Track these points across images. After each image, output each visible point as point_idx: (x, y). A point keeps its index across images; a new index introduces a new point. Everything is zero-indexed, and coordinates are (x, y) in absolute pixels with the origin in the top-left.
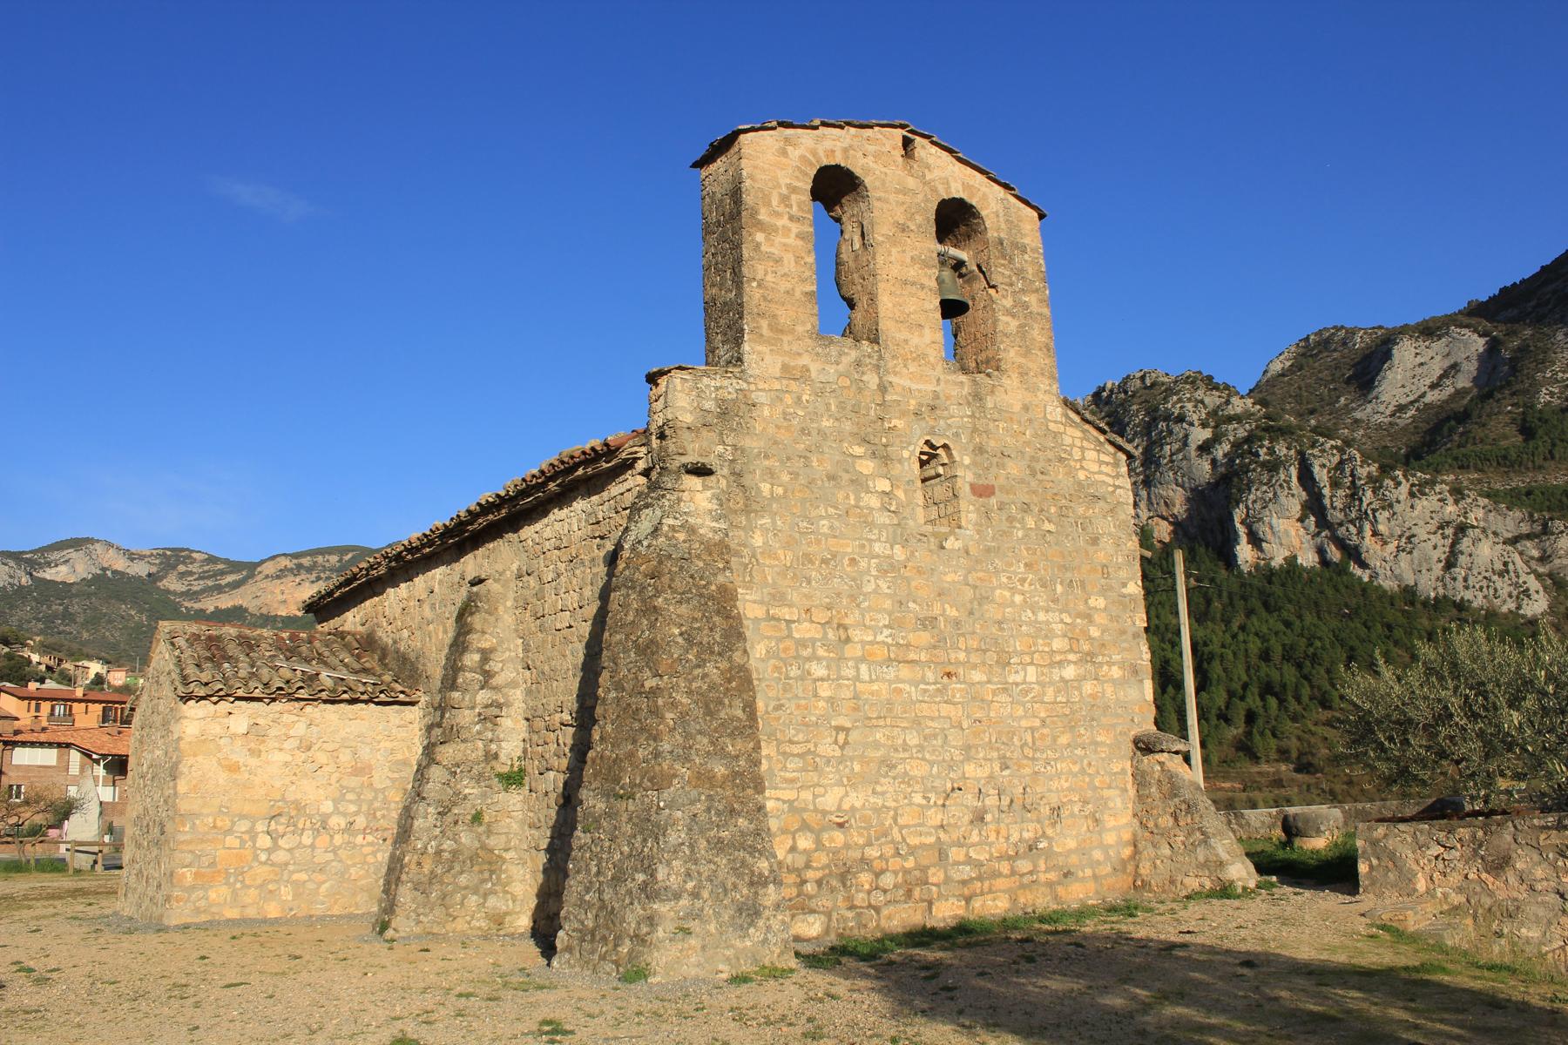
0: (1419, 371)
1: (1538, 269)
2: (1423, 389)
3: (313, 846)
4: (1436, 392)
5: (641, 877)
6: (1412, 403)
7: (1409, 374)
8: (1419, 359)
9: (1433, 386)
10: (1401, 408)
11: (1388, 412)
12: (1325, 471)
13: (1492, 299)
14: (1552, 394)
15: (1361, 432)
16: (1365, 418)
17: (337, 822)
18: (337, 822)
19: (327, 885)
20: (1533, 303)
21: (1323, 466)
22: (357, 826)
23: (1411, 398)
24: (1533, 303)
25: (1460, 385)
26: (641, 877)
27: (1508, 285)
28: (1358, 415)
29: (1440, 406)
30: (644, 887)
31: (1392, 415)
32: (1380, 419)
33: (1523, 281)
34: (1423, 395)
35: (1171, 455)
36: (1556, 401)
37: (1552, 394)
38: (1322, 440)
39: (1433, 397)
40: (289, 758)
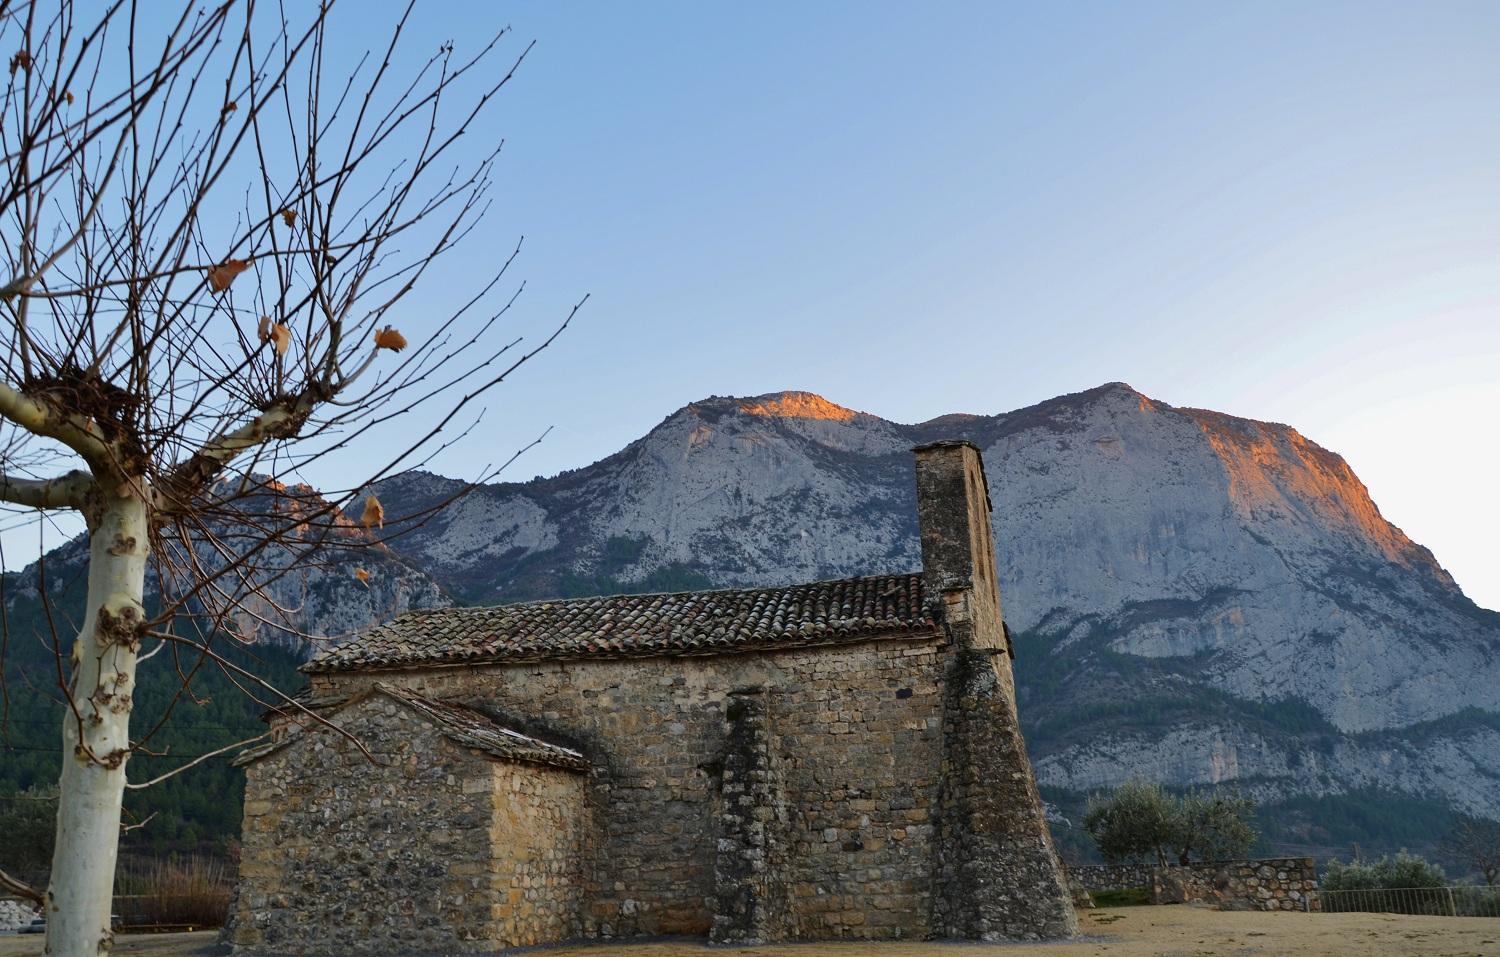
0: (486, 524)
1: (591, 463)
2: (486, 542)
3: (545, 887)
4: (497, 546)
5: (1043, 884)
6: (476, 551)
7: (478, 526)
8: (488, 516)
9: (496, 541)
10: (467, 554)
11: (455, 555)
12: (408, 598)
13: (554, 479)
14: (586, 566)
15: (430, 568)
16: (435, 556)
17: (555, 866)
18: (555, 866)
19: (551, 918)
20: (583, 490)
21: (408, 593)
22: (563, 871)
23: (476, 547)
24: (583, 490)
25: (516, 544)
26: (1043, 884)
27: (567, 470)
28: (429, 552)
29: (499, 559)
30: (1048, 889)
31: (458, 558)
32: (444, 559)
33: (578, 470)
34: (486, 547)
35: (269, 558)
36: (588, 573)
37: (586, 566)
38: (409, 570)
39: (495, 550)
40: (536, 813)
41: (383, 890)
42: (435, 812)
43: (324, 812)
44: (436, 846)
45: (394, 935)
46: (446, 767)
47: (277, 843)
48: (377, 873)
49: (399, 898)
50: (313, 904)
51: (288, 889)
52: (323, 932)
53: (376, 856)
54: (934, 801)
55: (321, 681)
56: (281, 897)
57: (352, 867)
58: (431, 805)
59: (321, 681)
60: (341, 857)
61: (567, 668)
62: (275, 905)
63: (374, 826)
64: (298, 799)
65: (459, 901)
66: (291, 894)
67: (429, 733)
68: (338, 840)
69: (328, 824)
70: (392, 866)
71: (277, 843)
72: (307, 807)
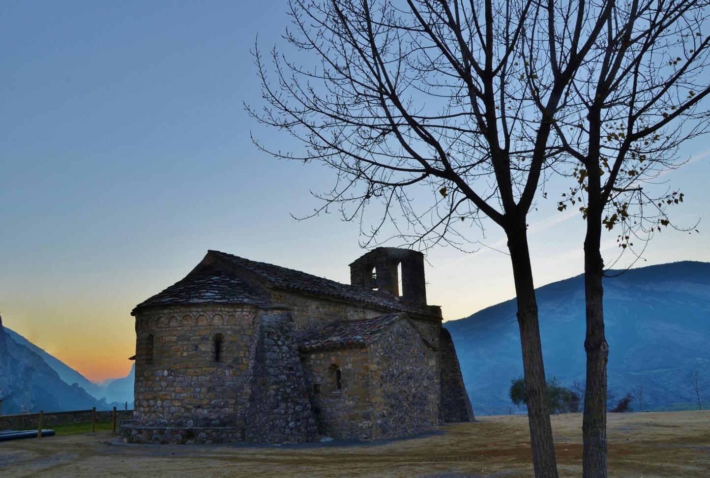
41: (413, 407)
42: (423, 373)
43: (394, 372)
44: (425, 387)
45: (417, 426)
46: (424, 354)
47: (381, 385)
48: (410, 399)
49: (417, 410)
50: (394, 414)
51: (386, 408)
52: (399, 427)
53: (410, 391)
54: (439, 377)
55: (276, 294)
56: (385, 412)
57: (404, 396)
58: (422, 370)
59: (276, 294)
60: (400, 392)
61: (365, 310)
62: (383, 416)
63: (409, 378)
64: (385, 364)
65: (431, 411)
66: (388, 410)
67: (418, 338)
68: (399, 383)
69: (396, 377)
70: (414, 396)
71: (381, 385)
72: (389, 368)
